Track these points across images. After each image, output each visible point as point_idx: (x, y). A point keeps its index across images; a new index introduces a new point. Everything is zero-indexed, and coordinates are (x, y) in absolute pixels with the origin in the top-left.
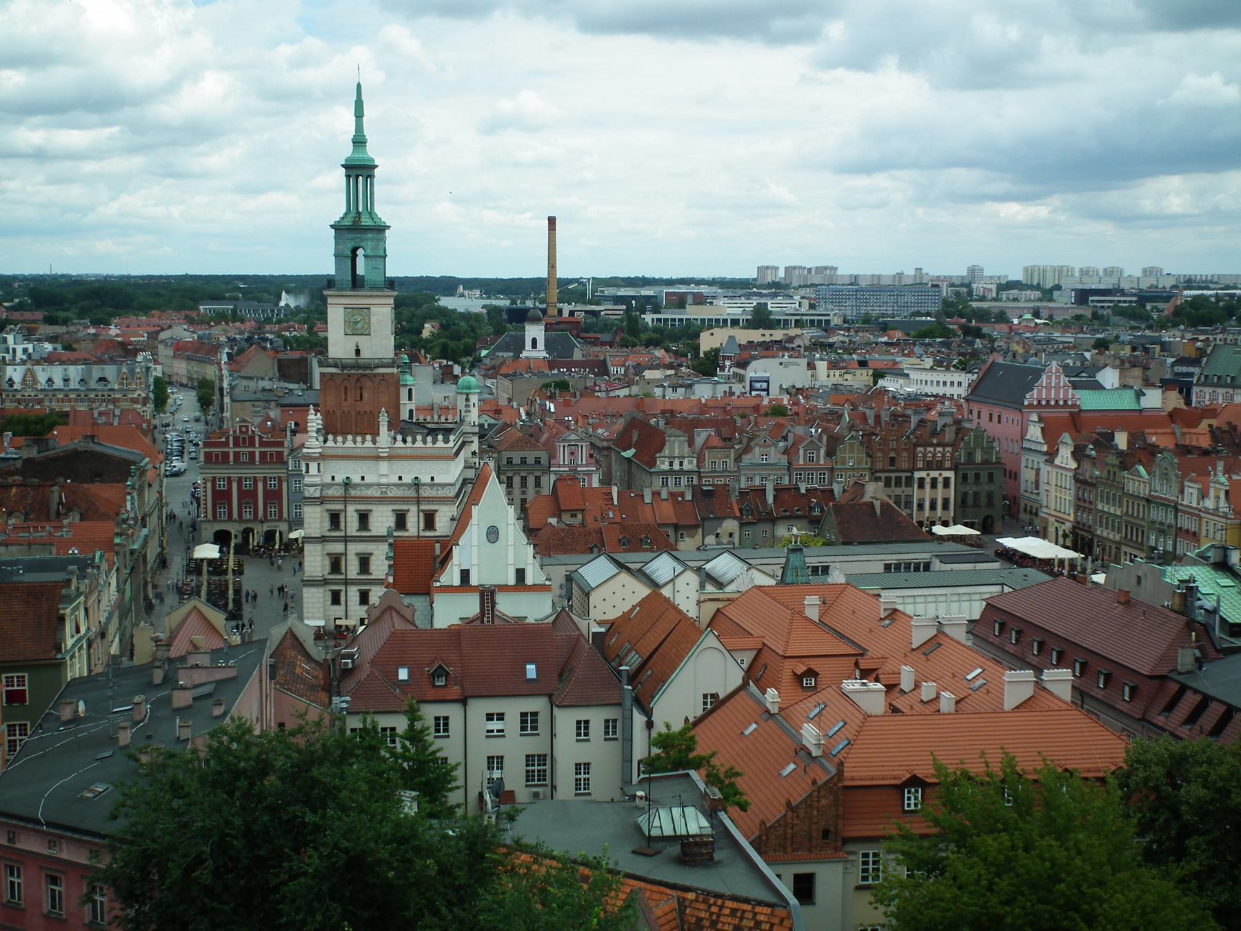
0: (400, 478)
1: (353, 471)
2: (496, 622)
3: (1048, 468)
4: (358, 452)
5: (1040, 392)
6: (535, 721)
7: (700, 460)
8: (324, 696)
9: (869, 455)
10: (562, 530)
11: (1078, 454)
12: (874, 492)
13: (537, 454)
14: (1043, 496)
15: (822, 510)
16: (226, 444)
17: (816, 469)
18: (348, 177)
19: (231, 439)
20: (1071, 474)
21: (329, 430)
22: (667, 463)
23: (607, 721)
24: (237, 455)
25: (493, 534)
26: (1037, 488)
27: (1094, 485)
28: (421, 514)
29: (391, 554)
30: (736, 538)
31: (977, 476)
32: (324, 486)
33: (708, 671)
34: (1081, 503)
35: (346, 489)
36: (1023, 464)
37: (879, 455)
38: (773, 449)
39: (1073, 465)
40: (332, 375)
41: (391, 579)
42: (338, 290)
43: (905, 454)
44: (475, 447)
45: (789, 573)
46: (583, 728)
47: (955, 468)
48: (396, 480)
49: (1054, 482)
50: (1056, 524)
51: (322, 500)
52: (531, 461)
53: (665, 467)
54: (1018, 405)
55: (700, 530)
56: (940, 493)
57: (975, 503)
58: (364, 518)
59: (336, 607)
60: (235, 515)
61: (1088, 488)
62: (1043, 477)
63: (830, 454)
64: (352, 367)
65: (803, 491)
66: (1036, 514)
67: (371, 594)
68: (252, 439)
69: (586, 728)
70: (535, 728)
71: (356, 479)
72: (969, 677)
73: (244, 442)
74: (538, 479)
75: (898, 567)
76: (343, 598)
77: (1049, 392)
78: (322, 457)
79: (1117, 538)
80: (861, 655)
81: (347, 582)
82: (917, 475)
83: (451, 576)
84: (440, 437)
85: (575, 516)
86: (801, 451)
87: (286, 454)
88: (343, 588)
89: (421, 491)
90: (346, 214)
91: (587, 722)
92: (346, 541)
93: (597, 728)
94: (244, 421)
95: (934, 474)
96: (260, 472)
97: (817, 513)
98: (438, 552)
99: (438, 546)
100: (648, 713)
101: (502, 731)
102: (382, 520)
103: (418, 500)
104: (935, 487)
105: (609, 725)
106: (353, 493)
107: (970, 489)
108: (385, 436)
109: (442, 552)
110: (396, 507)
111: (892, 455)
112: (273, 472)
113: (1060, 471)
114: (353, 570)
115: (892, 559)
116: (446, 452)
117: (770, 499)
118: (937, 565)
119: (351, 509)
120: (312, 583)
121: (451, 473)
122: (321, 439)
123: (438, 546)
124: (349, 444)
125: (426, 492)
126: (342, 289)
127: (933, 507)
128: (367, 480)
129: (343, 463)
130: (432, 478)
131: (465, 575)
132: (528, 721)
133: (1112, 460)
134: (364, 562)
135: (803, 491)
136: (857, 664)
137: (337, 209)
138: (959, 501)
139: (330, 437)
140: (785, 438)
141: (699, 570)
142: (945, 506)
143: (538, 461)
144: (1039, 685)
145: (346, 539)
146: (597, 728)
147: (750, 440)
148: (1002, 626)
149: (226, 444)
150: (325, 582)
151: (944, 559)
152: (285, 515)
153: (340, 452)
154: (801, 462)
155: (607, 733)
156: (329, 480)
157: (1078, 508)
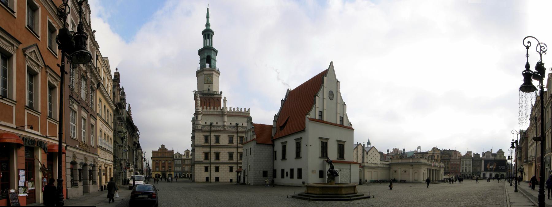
51: (201, 131)
59: (207, 173)
71: (215, 124)
76: (209, 169)
81: (211, 163)
88: (209, 165)
102: (224, 140)
103: (237, 132)
106: (213, 129)
110: (229, 135)
114: (213, 158)
119: (212, 135)
125: (240, 129)
134: (217, 156)
145: (211, 147)
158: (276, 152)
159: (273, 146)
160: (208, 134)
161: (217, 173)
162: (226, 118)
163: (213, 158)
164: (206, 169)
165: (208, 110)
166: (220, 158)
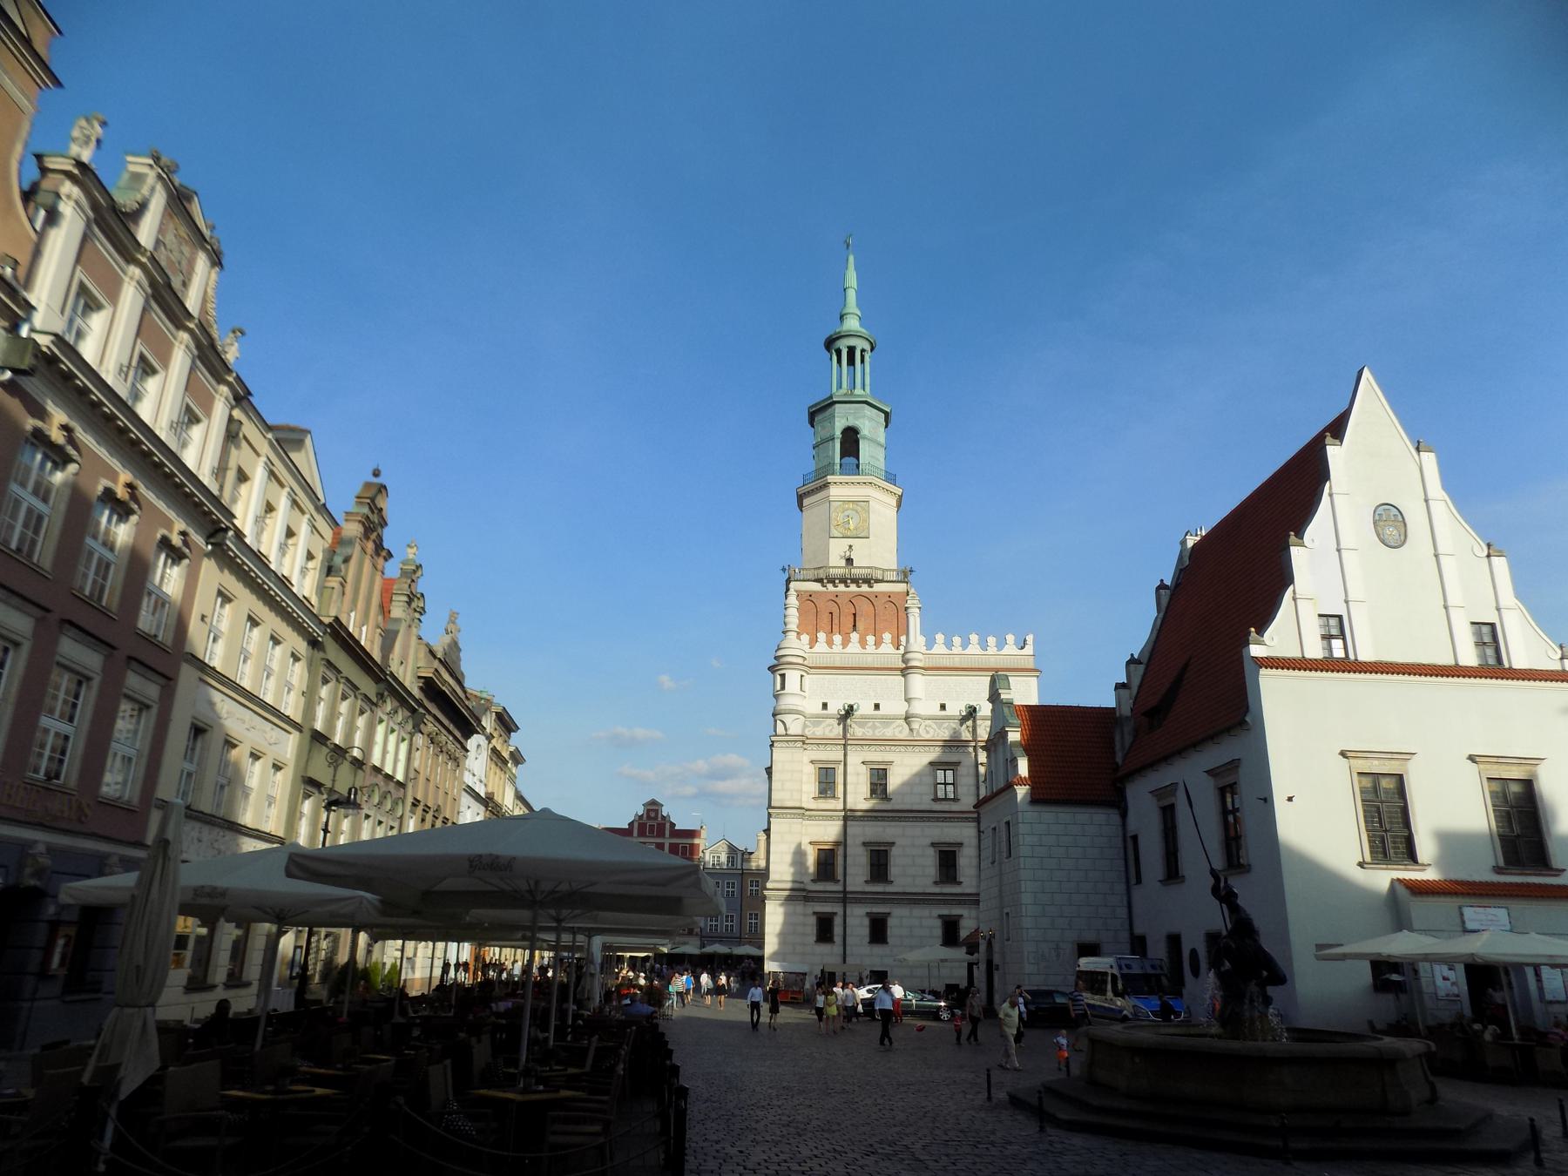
4: (869, 661)
25: (1390, 524)
48: (937, 711)
51: (804, 741)
59: (824, 948)
67: (891, 922)
68: (661, 828)
71: (864, 708)
73: (652, 831)
76: (838, 930)
81: (845, 898)
88: (838, 909)
122: (805, 638)
131: (1336, 626)
158: (1135, 838)
159: (1118, 803)
161: (878, 949)
162: (917, 680)
166: (894, 871)
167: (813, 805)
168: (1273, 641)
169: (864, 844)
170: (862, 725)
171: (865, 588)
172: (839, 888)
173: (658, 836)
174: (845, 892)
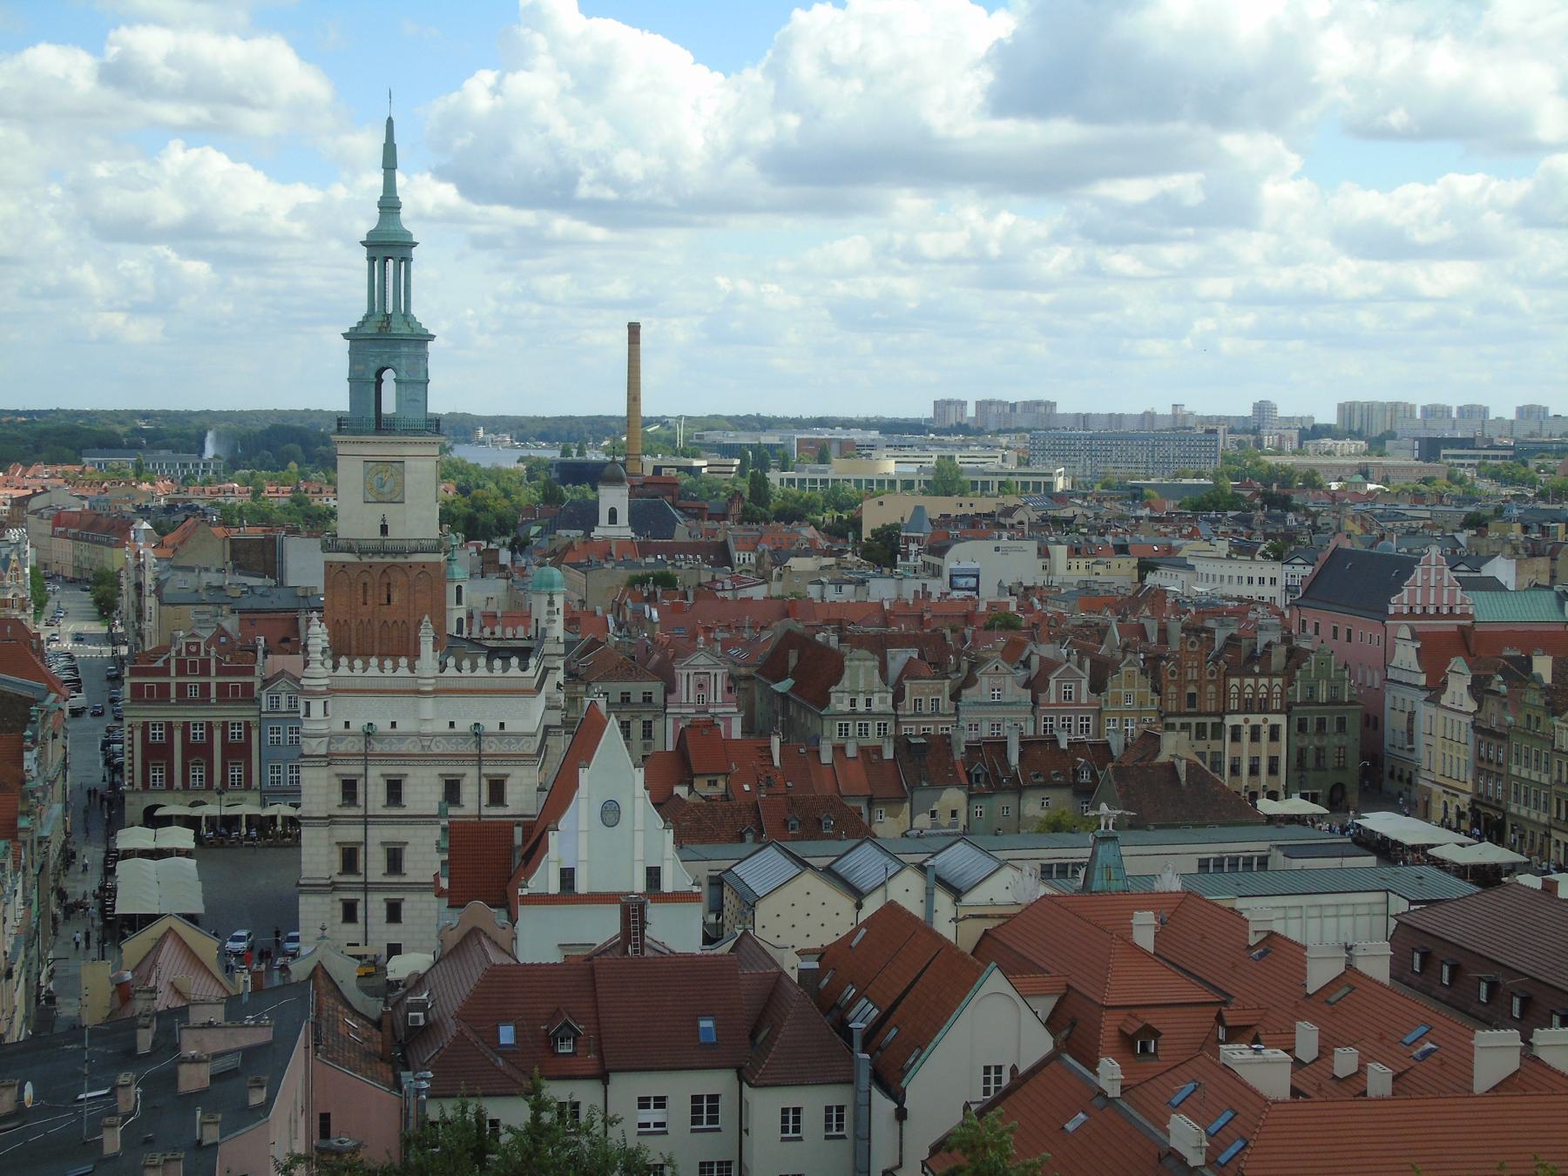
0: (452, 724)
1: (378, 712)
2: (648, 953)
3: (1431, 710)
4: (387, 684)
5: (1412, 594)
6: (713, 1109)
7: (898, 697)
8: (384, 1069)
9: (1156, 690)
10: (696, 805)
11: (1479, 689)
12: (1175, 746)
13: (648, 686)
14: (1422, 752)
15: (1094, 775)
16: (165, 671)
17: (1075, 712)
18: (372, 259)
19: (173, 662)
20: (1468, 720)
21: (339, 649)
22: (847, 702)
23: (828, 1109)
24: (181, 688)
25: (611, 813)
26: (1411, 742)
27: (1502, 736)
28: (485, 782)
29: (445, 845)
30: (962, 819)
31: (1321, 723)
32: (333, 737)
33: (995, 1029)
34: (1484, 765)
35: (367, 743)
36: (1388, 703)
37: (1172, 689)
38: (1009, 679)
39: (1471, 706)
40: (344, 565)
41: (444, 883)
42: (354, 433)
43: (1211, 688)
44: (560, 676)
45: (1097, 874)
46: (791, 1120)
47: (1287, 709)
48: (445, 728)
49: (1443, 735)
50: (1445, 797)
51: (330, 759)
52: (637, 697)
53: (845, 707)
54: (1383, 615)
55: (907, 805)
56: (1264, 749)
57: (1318, 760)
58: (394, 790)
59: (350, 927)
60: (178, 782)
61: (1495, 742)
62: (1421, 725)
63: (1097, 686)
64: (376, 552)
65: (1064, 745)
66: (1409, 781)
67: (404, 906)
68: (205, 666)
69: (797, 1120)
70: (713, 1120)
71: (383, 726)
72: (1408, 1040)
73: (193, 668)
74: (647, 726)
75: (1219, 864)
76: (360, 913)
77: (1426, 595)
78: (332, 691)
79: (1544, 819)
80: (1224, 1003)
81: (366, 888)
82: (1230, 721)
83: (545, 879)
84: (514, 661)
85: (715, 783)
86: (1052, 684)
87: (257, 686)
88: (360, 896)
89: (484, 746)
90: (367, 317)
91: (797, 1111)
92: (366, 823)
93: (813, 1122)
94: (193, 635)
95: (1256, 719)
96: (217, 714)
97: (1086, 778)
98: (518, 840)
99: (518, 831)
100: (898, 1096)
101: (663, 1125)
102: (423, 792)
103: (479, 759)
104: (1255, 741)
105: (834, 1116)
106: (377, 747)
107: (1311, 742)
108: (428, 657)
109: (525, 840)
110: (444, 770)
111: (1192, 689)
112: (237, 714)
113: (1451, 715)
114: (375, 866)
115: (1211, 851)
116: (524, 685)
117: (1014, 758)
118: (1278, 860)
119: (375, 772)
120: (316, 889)
121: (528, 716)
122: (329, 663)
123: (518, 831)
124: (373, 671)
125: (489, 747)
126: (361, 433)
127: (1254, 770)
128: (400, 728)
129: (362, 701)
130: (502, 725)
131: (567, 876)
132: (704, 1109)
133: (1533, 697)
134: (395, 859)
135: (1064, 745)
136: (1219, 1019)
137: (356, 308)
138: (1294, 759)
139: (344, 661)
140: (1026, 664)
141: (921, 868)
142: (1273, 770)
143: (647, 698)
144: (1528, 1054)
145: (366, 820)
146: (813, 1122)
147: (973, 666)
148: (1426, 957)
149: (165, 671)
150: (334, 887)
151: (1291, 852)
152: (255, 781)
153: (358, 684)
154: (1053, 701)
155: (828, 1127)
156: (340, 727)
157: (1479, 771)
160: (354, 769)
161: (394, 927)
163: (375, 866)
164: (349, 912)
165: (358, 672)
166: (407, 865)
167: (338, 812)
168: (534, 885)
169: (383, 844)
170: (381, 742)
171: (400, 559)
172: (362, 879)
173: (201, 675)
174: (366, 883)
